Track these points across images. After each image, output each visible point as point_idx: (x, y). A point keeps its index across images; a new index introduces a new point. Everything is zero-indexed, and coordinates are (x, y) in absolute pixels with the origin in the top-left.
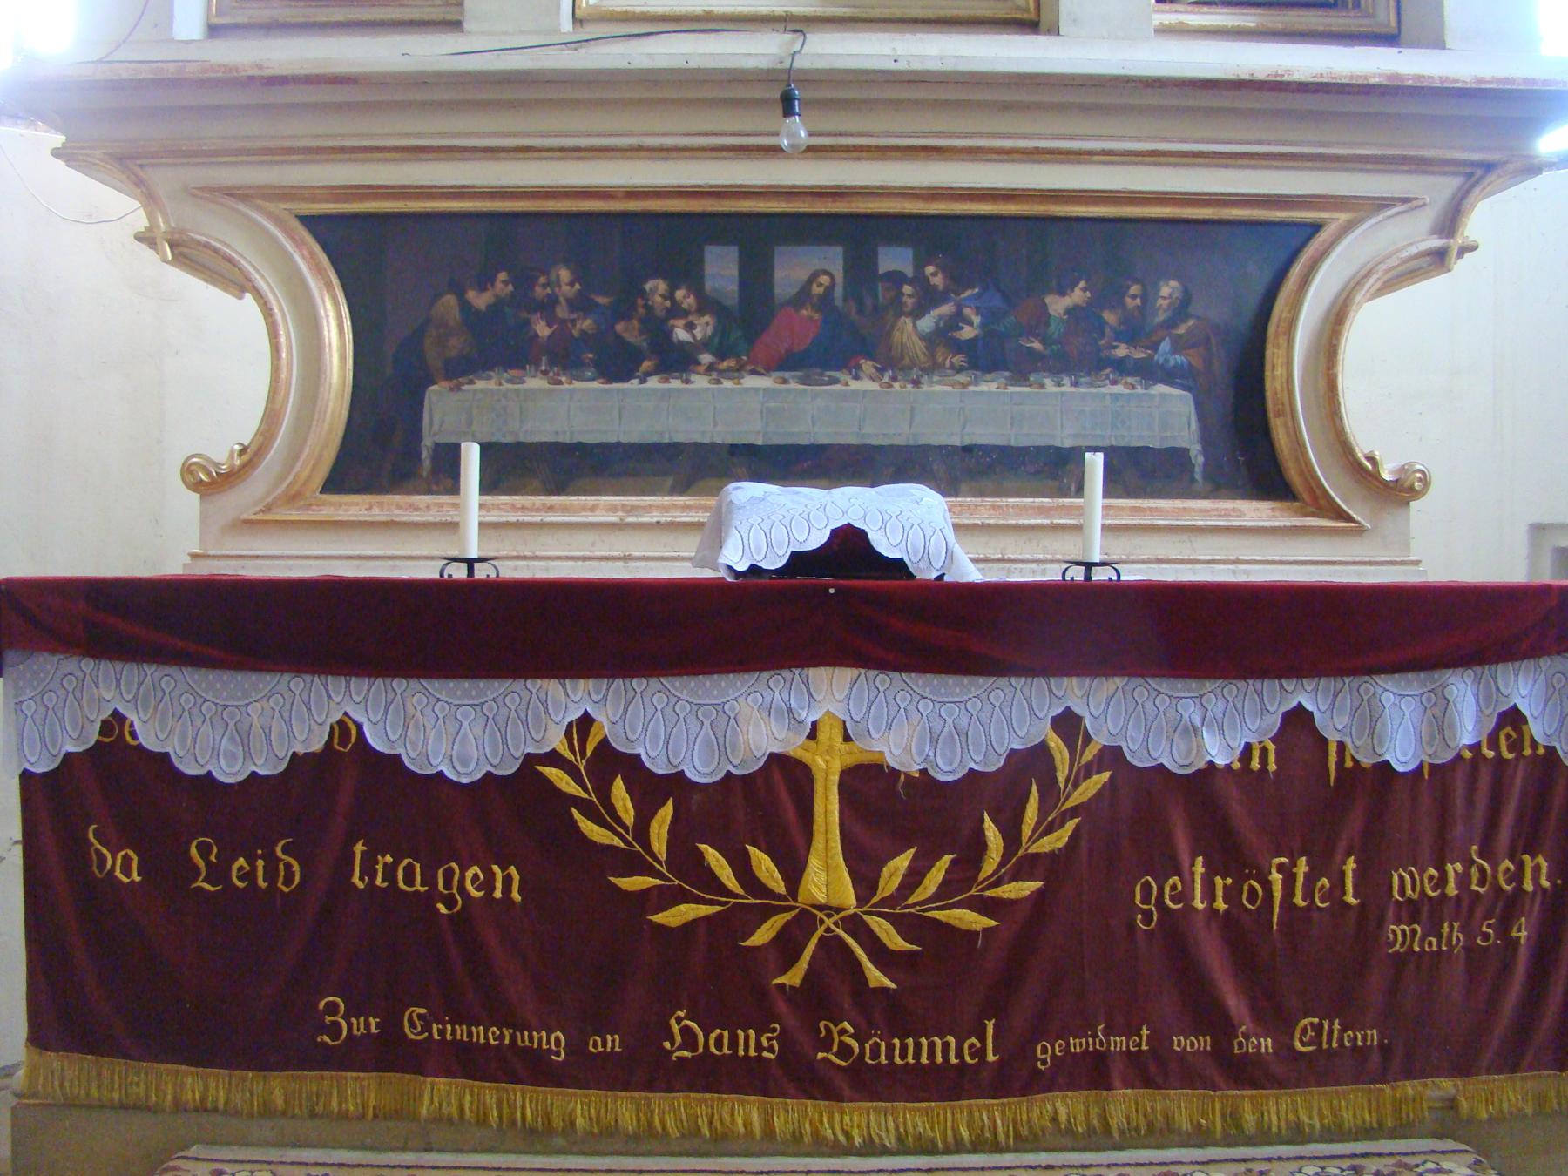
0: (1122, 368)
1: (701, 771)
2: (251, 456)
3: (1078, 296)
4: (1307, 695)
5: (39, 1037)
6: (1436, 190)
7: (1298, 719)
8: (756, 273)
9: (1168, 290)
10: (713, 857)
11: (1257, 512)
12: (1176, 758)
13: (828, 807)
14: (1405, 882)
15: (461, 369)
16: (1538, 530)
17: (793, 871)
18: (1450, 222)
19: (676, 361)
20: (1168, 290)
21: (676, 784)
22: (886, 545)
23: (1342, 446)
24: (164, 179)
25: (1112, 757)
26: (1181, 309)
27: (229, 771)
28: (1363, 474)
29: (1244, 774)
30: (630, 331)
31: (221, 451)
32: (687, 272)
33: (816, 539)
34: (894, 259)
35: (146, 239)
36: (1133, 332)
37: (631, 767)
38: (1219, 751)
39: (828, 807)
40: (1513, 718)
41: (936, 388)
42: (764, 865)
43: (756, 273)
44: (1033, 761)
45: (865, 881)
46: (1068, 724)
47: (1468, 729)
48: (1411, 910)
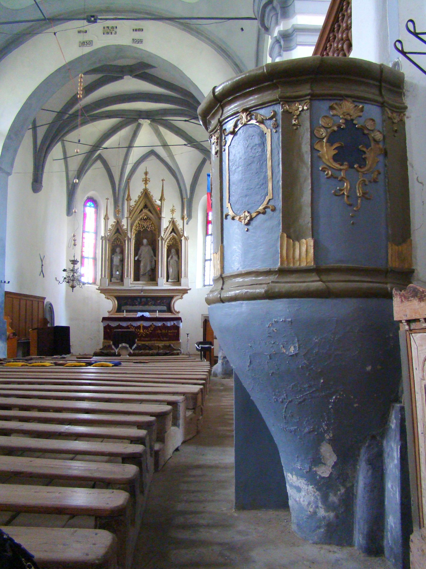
0: (162, 305)
1: (136, 326)
2: (112, 310)
3: (159, 301)
4: (164, 322)
5: (105, 338)
6: (181, 294)
7: (164, 324)
8: (141, 300)
9: (165, 301)
10: (136, 330)
11: (170, 314)
12: (158, 325)
13: (142, 327)
14: (169, 331)
15: (124, 305)
16: (202, 315)
17: (140, 330)
18: (182, 296)
19: (136, 305)
20: (165, 301)
21: (134, 326)
22: (145, 315)
23: (174, 310)
24: (106, 294)
25: (155, 325)
26: (166, 302)
27: (114, 326)
28: (176, 312)
29: (161, 326)
30: (134, 303)
31: (110, 310)
32: (137, 300)
33: (141, 315)
34: (149, 299)
35: (105, 298)
36: (163, 303)
37: (132, 326)
38: (160, 325)
39: (142, 327)
40: (175, 324)
41: (151, 307)
42: (139, 330)
43: (141, 300)
44: (151, 326)
45: (143, 331)
46: (153, 324)
47: (172, 324)
48: (170, 333)
